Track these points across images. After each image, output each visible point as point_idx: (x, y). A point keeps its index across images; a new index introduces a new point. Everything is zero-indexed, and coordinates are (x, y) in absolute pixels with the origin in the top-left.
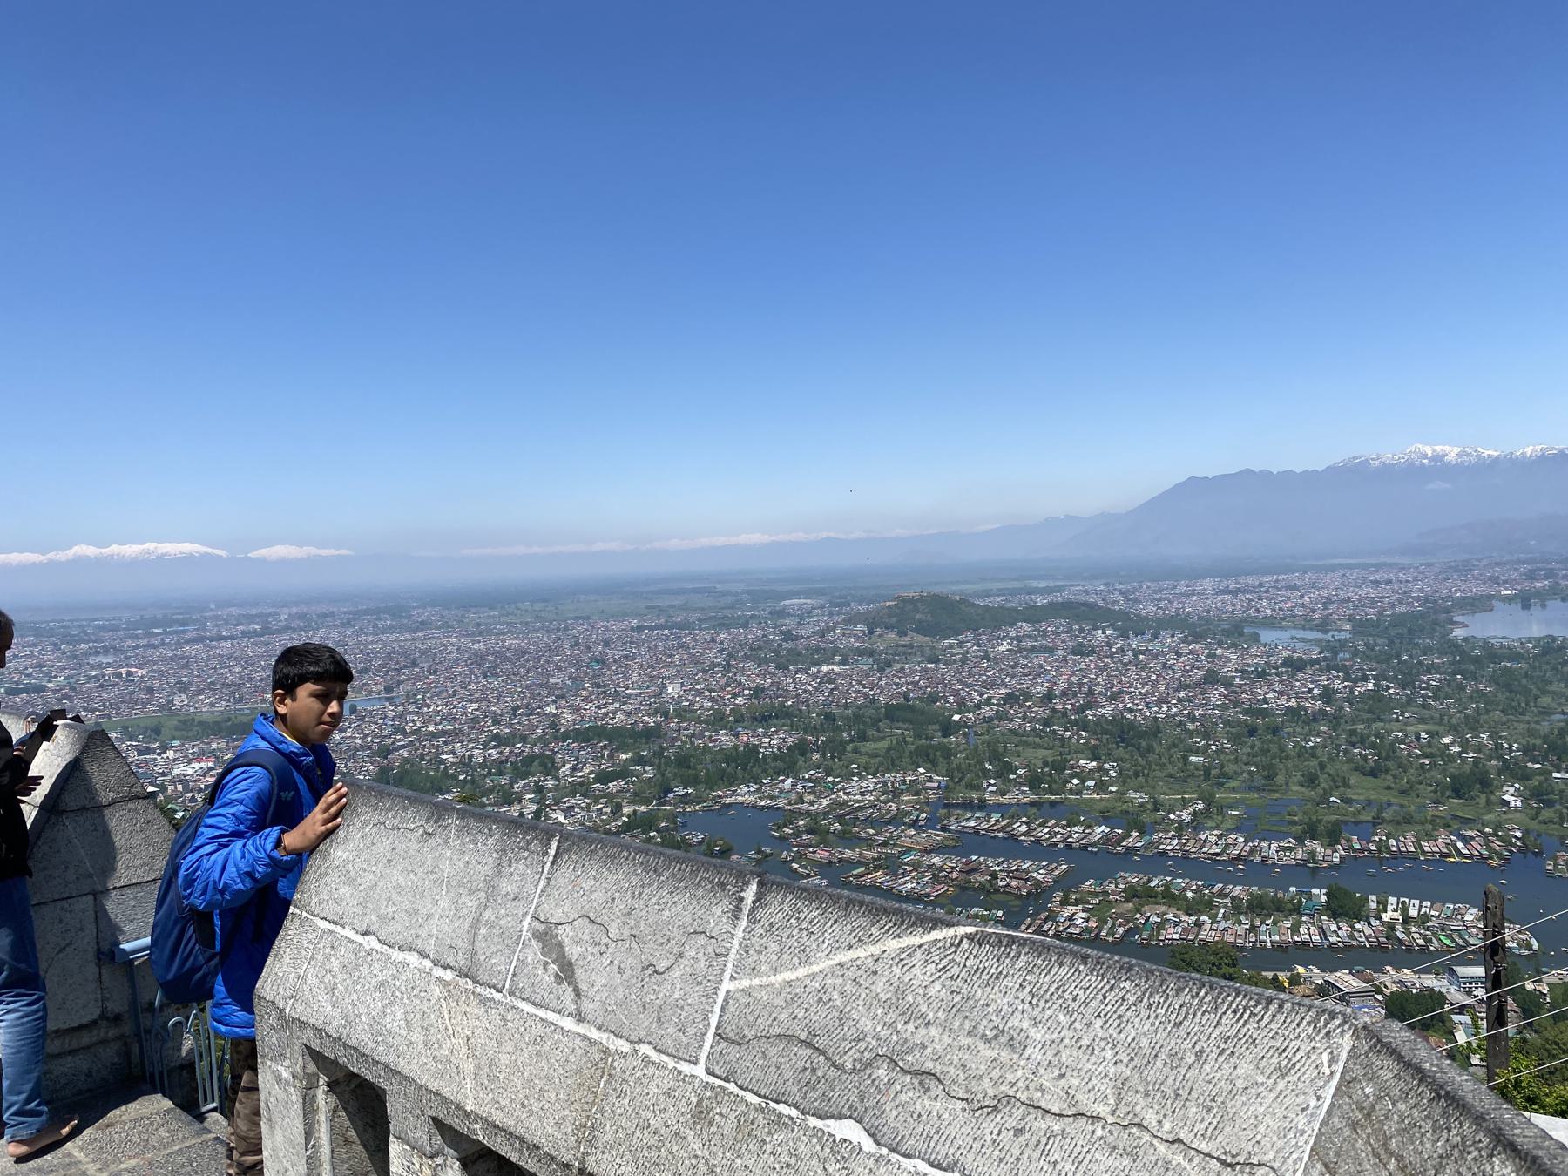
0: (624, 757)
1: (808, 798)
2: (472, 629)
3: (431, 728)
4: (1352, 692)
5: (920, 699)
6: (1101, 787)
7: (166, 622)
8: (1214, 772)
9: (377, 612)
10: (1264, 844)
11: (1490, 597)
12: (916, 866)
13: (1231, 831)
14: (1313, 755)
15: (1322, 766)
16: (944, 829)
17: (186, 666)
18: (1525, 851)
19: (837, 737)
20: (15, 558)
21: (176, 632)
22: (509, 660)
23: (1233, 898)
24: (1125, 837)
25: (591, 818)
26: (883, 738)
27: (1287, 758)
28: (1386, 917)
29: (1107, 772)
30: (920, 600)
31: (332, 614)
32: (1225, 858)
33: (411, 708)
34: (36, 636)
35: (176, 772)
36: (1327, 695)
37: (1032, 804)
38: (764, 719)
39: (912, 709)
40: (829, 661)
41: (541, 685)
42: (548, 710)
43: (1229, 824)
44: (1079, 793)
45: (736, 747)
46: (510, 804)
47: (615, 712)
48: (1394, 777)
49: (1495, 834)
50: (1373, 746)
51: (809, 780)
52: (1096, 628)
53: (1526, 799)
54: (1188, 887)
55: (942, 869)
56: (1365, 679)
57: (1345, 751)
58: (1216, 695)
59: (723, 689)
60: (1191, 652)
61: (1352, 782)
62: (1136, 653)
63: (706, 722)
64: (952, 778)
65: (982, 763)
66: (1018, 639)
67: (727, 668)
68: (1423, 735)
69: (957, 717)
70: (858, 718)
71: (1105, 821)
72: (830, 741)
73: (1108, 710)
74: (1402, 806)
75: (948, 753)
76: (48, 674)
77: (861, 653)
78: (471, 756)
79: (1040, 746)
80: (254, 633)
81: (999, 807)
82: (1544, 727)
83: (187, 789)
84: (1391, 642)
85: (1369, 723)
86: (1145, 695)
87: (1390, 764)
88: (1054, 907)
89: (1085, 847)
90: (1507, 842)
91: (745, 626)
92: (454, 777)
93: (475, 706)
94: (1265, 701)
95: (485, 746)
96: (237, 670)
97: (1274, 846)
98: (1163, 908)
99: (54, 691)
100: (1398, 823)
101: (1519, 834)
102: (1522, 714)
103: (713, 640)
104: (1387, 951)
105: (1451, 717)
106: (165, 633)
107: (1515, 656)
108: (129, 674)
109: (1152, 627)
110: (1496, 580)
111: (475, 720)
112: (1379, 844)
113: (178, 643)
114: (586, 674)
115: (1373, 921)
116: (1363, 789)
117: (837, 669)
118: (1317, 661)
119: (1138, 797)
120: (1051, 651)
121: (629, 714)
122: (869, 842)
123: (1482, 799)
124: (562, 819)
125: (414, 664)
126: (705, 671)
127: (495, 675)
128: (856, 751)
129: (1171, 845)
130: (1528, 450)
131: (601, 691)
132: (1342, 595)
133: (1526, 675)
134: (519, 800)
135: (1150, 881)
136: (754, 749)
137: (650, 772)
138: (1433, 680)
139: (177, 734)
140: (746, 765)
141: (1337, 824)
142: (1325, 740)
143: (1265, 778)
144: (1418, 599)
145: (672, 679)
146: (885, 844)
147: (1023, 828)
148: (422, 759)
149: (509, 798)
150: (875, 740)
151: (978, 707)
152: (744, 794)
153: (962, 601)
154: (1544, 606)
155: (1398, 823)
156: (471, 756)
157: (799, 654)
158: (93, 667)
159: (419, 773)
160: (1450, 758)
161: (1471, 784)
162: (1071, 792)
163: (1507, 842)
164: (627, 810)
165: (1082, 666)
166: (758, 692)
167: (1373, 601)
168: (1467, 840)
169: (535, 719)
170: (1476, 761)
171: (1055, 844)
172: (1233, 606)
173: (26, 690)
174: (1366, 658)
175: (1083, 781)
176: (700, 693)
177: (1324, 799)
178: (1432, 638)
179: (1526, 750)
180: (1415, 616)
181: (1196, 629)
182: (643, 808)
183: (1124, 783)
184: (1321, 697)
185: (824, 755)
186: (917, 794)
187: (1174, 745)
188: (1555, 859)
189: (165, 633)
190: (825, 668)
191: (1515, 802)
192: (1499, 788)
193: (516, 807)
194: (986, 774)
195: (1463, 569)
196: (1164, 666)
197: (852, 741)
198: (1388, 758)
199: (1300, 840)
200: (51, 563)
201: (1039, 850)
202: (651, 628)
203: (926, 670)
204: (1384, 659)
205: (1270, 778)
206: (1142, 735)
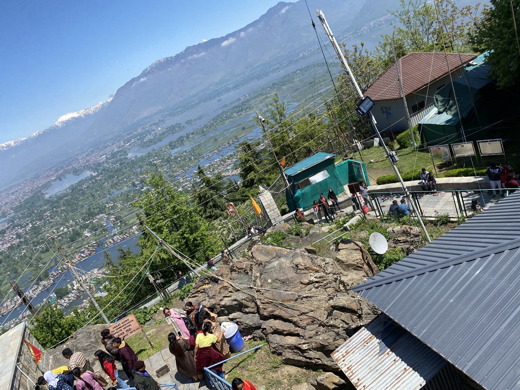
4: (26, 231)
11: (49, 182)
13: (13, 297)
18: (98, 246)
23: (27, 316)
27: (18, 262)
28: (75, 288)
36: (19, 236)
49: (89, 246)
50: (42, 243)
53: (91, 232)
56: (27, 224)
57: (35, 249)
68: (55, 231)
82: (84, 211)
84: (29, 209)
85: (37, 237)
97: (31, 291)
101: (94, 242)
102: (77, 210)
107: (66, 195)
110: (48, 176)
112: (61, 269)
115: (73, 291)
118: (8, 228)
130: (34, 134)
132: (4, 202)
143: (15, 273)
144: (29, 192)
154: (65, 178)
160: (66, 233)
161: (75, 236)
167: (15, 200)
168: (83, 252)
170: (73, 230)
177: (38, 268)
179: (83, 219)
180: (31, 198)
184: (17, 238)
188: (106, 243)
191: (89, 235)
192: (83, 233)
195: (37, 177)
199: (37, 284)
205: (16, 272)
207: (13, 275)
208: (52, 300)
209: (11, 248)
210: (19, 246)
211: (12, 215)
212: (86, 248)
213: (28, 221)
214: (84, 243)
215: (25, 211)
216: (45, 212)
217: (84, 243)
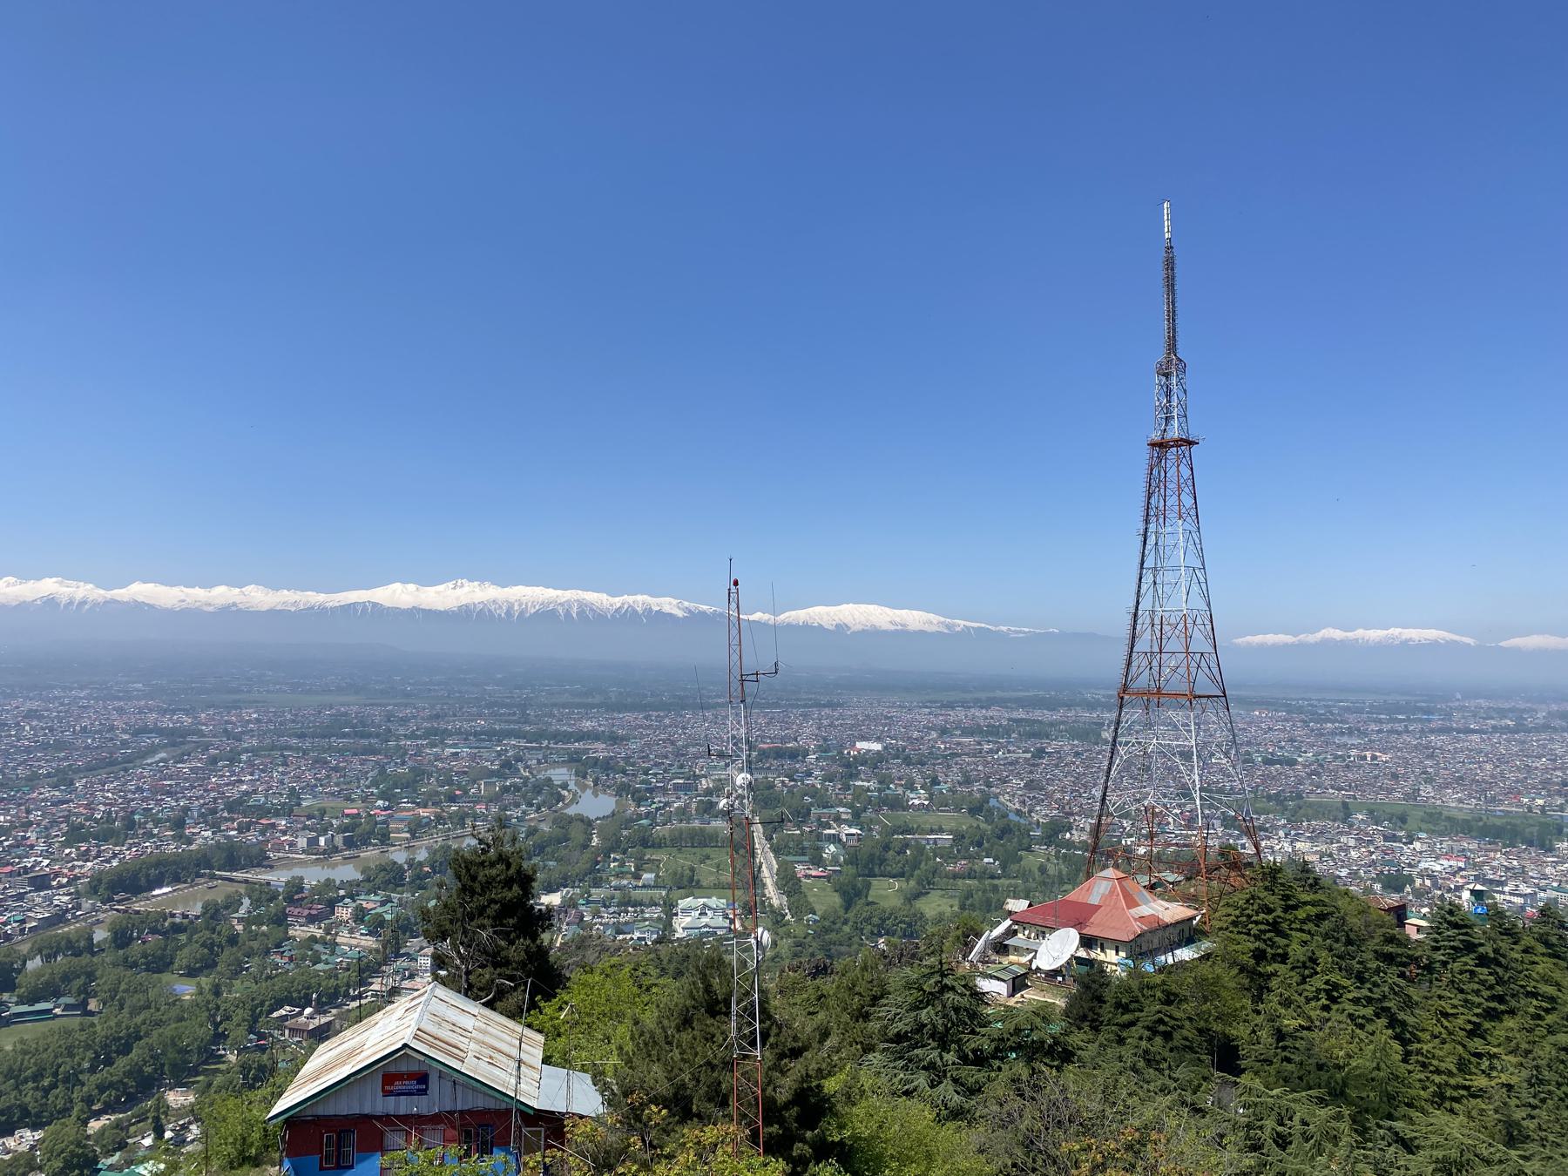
21: (1420, 720)
34: (1288, 712)
35: (1423, 865)
83: (1436, 886)
96: (1488, 767)
99: (1305, 766)
108: (1374, 758)
113: (1422, 731)
139: (1424, 826)
158: (1339, 746)
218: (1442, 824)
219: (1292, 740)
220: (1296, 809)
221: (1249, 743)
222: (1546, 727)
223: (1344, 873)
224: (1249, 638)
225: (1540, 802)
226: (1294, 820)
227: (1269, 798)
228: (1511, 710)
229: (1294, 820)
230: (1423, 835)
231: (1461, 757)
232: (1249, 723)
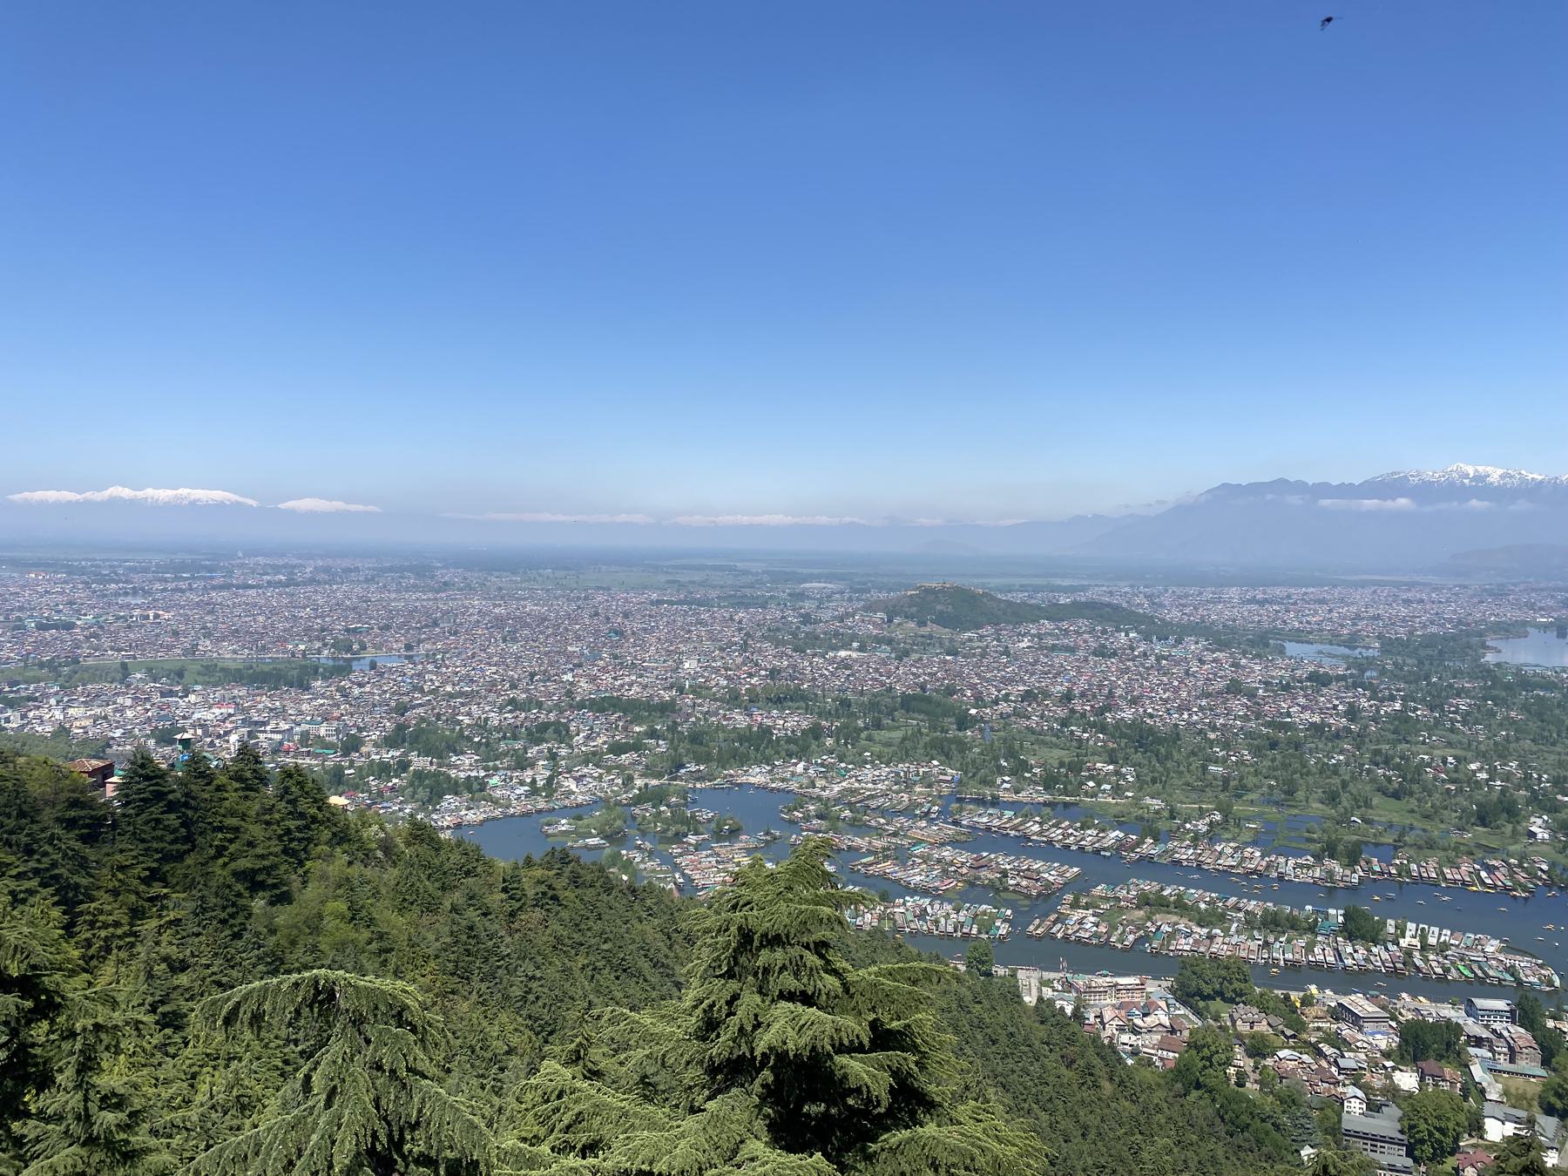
0: (637, 729)
1: (820, 783)
2: (494, 593)
3: (449, 688)
4: (1378, 711)
5: (936, 691)
6: (1117, 791)
7: (194, 567)
8: (1232, 783)
9: (401, 569)
10: (1282, 860)
12: (926, 859)
13: (1247, 844)
14: (1336, 773)
15: (1344, 784)
16: (956, 823)
17: (209, 613)
19: (852, 724)
20: (52, 495)
21: (204, 578)
22: (528, 625)
24: (1139, 843)
25: (602, 789)
26: (898, 728)
29: (1123, 776)
30: (942, 591)
31: (357, 569)
32: (1240, 871)
33: (430, 667)
34: (69, 573)
35: (196, 716)
36: (1353, 713)
37: (1045, 804)
38: (778, 701)
39: (928, 700)
40: (846, 646)
41: (559, 653)
42: (565, 678)
43: (1246, 837)
44: (1094, 795)
45: (750, 727)
46: (523, 769)
47: (631, 685)
48: (1419, 800)
49: (1520, 866)
50: (1398, 767)
51: (822, 765)
52: (1119, 630)
54: (1202, 898)
55: (952, 864)
56: (1392, 698)
57: (1369, 771)
58: (1238, 705)
59: (738, 668)
60: (1215, 660)
61: (1375, 802)
62: (1159, 658)
63: (721, 700)
64: (966, 773)
65: (996, 759)
66: (1040, 637)
67: (744, 647)
68: (1450, 759)
69: (973, 711)
70: (873, 706)
71: (1120, 825)
72: (845, 726)
73: (1128, 714)
74: (1424, 830)
75: (963, 747)
76: (78, 611)
77: (879, 640)
78: (487, 719)
79: (1056, 746)
80: (280, 584)
81: (1012, 805)
84: (1421, 663)
85: (1394, 743)
86: (1166, 701)
87: (1415, 787)
88: (1064, 909)
89: (1097, 852)
90: (1532, 875)
91: (764, 607)
92: (469, 739)
93: (494, 669)
94: (1289, 715)
95: (501, 708)
96: (261, 619)
97: (1291, 862)
98: (1174, 918)
99: (83, 629)
100: (1420, 848)
101: (1545, 867)
102: (1553, 744)
103: (731, 619)
104: (1401, 977)
105: (1480, 743)
106: (193, 578)
107: (1549, 685)
108: (157, 616)
109: (1181, 632)
111: (493, 683)
112: (1400, 868)
114: (605, 644)
116: (1386, 811)
117: (854, 655)
119: (1156, 804)
120: (1072, 650)
121: (645, 687)
122: (879, 831)
123: (1510, 827)
124: (573, 787)
125: (435, 624)
126: (722, 649)
127: (515, 640)
128: (869, 739)
129: (1185, 854)
131: (618, 662)
133: (1559, 705)
134: (532, 765)
135: (1162, 889)
136: (767, 731)
137: (663, 746)
138: (1463, 704)
139: (200, 679)
140: (758, 745)
141: (1358, 844)
142: (1347, 759)
143: (1285, 793)
145: (690, 654)
146: (895, 834)
147: (1036, 828)
148: (438, 719)
149: (522, 763)
150: (890, 729)
151: (996, 702)
152: (757, 775)
153: (985, 595)
155: (1420, 848)
156: (487, 719)
157: (817, 638)
158: (121, 607)
159: (435, 733)
160: (1478, 784)
161: (1496, 813)
162: (1086, 794)
163: (1532, 875)
164: (639, 782)
165: (1103, 667)
166: (774, 673)
168: (1491, 870)
169: (552, 687)
170: (1504, 791)
171: (1067, 847)
172: (1262, 616)
173: (56, 627)
174: (1395, 677)
175: (1099, 784)
176: (717, 671)
177: (1343, 820)
178: (1463, 661)
181: (1221, 638)
182: (655, 782)
183: (1141, 789)
185: (838, 741)
186: (930, 786)
187: (1193, 753)
189: (193, 578)
190: (843, 654)
191: (1542, 834)
192: (1527, 818)
193: (529, 772)
194: (1000, 771)
196: (1187, 673)
197: (866, 728)
198: (1412, 781)
199: (1318, 858)
200: (87, 502)
201: (1049, 851)
202: (671, 603)
203: (945, 662)
204: (1411, 679)
205: (1290, 793)
206: (1160, 741)
207: (1278, 795)
208: (1326, 924)
209: (1317, 729)
210: (1337, 736)
211: (1370, 653)
212: (1509, 864)
213: (1398, 690)
214: (1512, 848)
215: (1409, 661)
216: (1458, 695)
217: (1512, 848)
218: (216, 675)
219: (71, 603)
220: (69, 674)
221: (21, 609)
222: (312, 581)
223: (118, 733)
224: (27, 494)
225: (302, 647)
226: (67, 687)
227: (42, 665)
228: (284, 566)
229: (67, 687)
230: (198, 688)
231: (237, 611)
232: (23, 587)
